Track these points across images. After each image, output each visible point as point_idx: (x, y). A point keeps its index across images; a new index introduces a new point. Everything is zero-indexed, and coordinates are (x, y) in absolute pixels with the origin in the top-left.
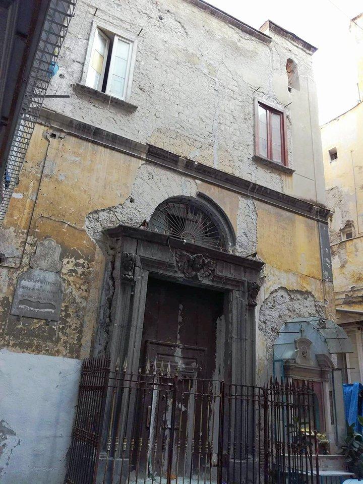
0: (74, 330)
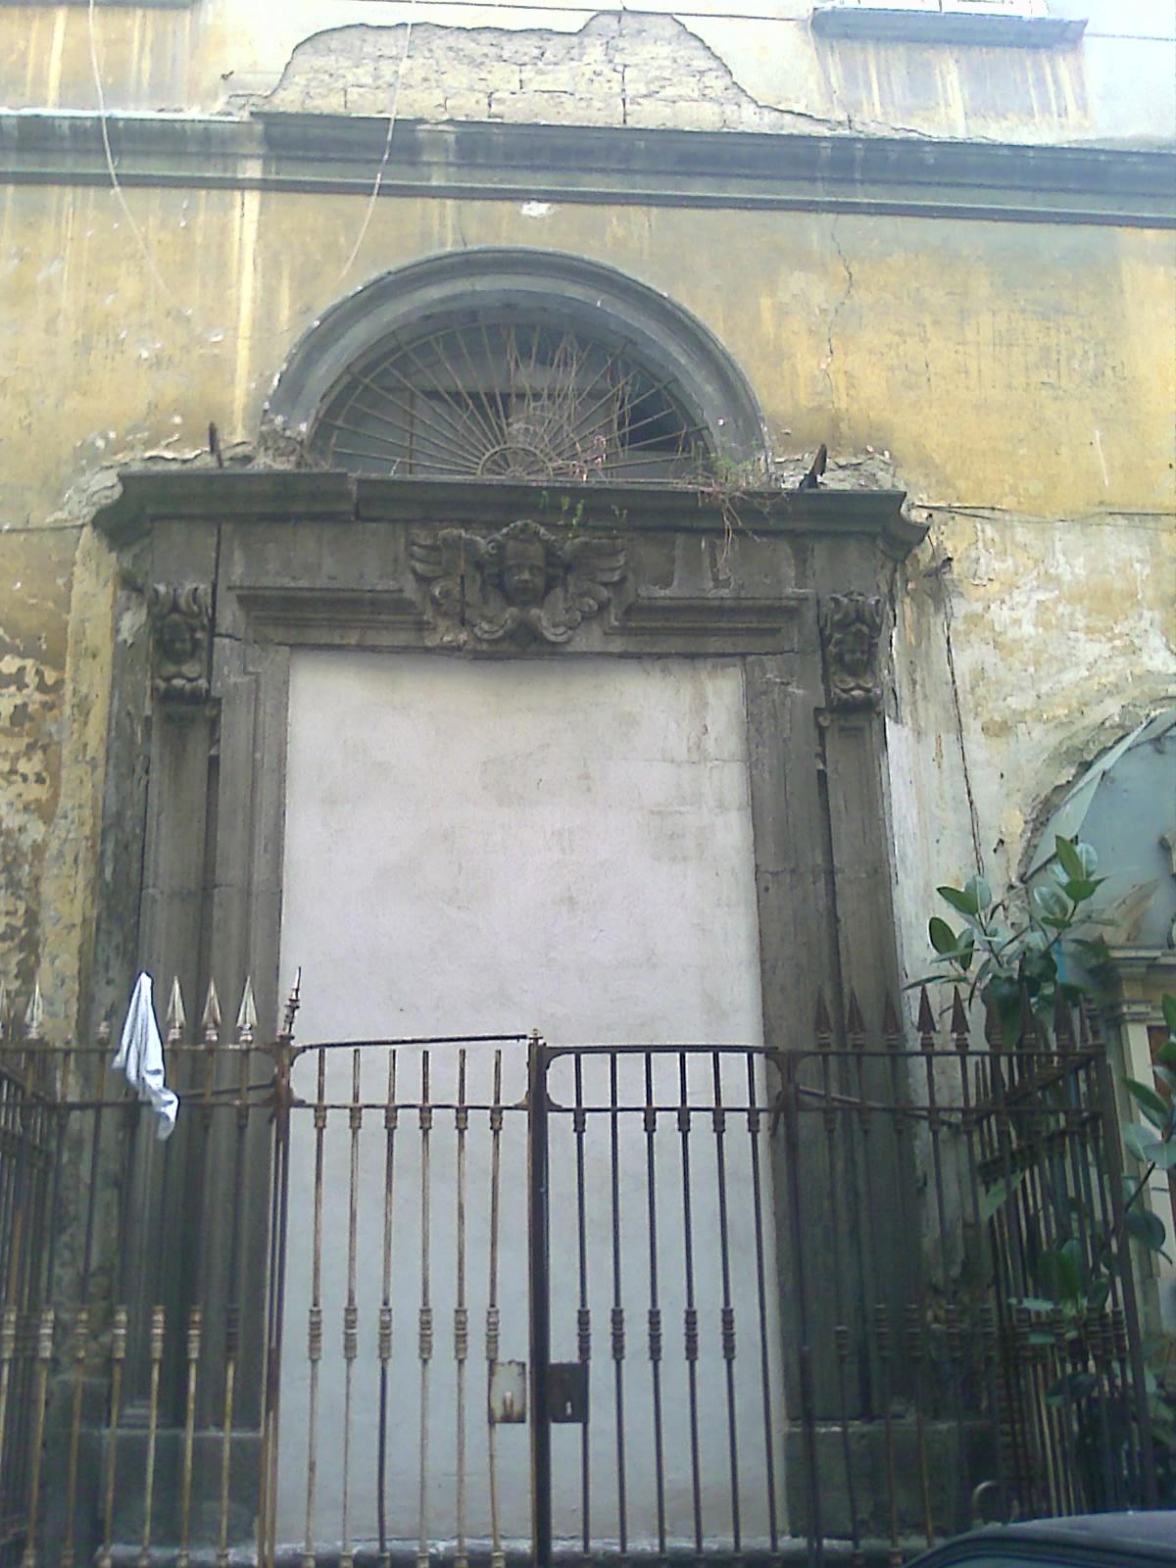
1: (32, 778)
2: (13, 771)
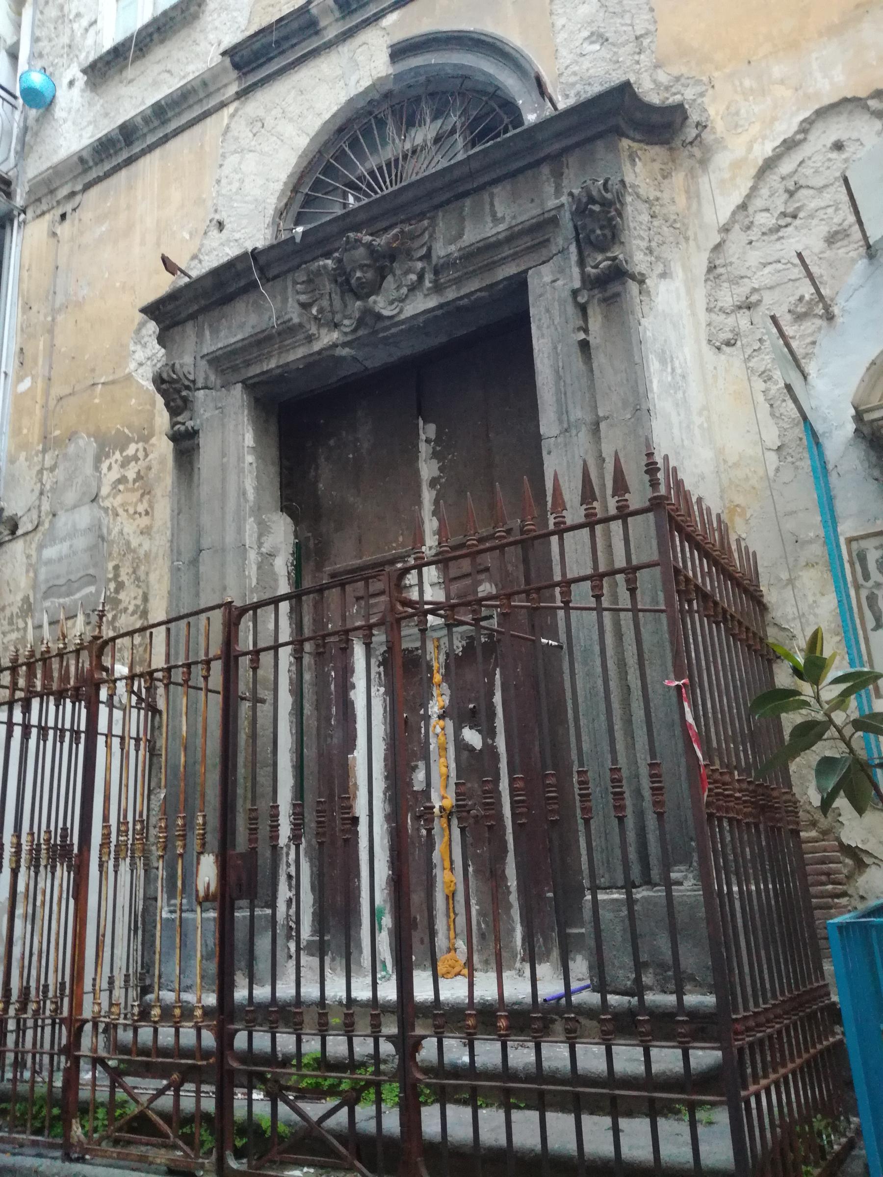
0: (133, 614)
1: (143, 513)
2: (135, 513)
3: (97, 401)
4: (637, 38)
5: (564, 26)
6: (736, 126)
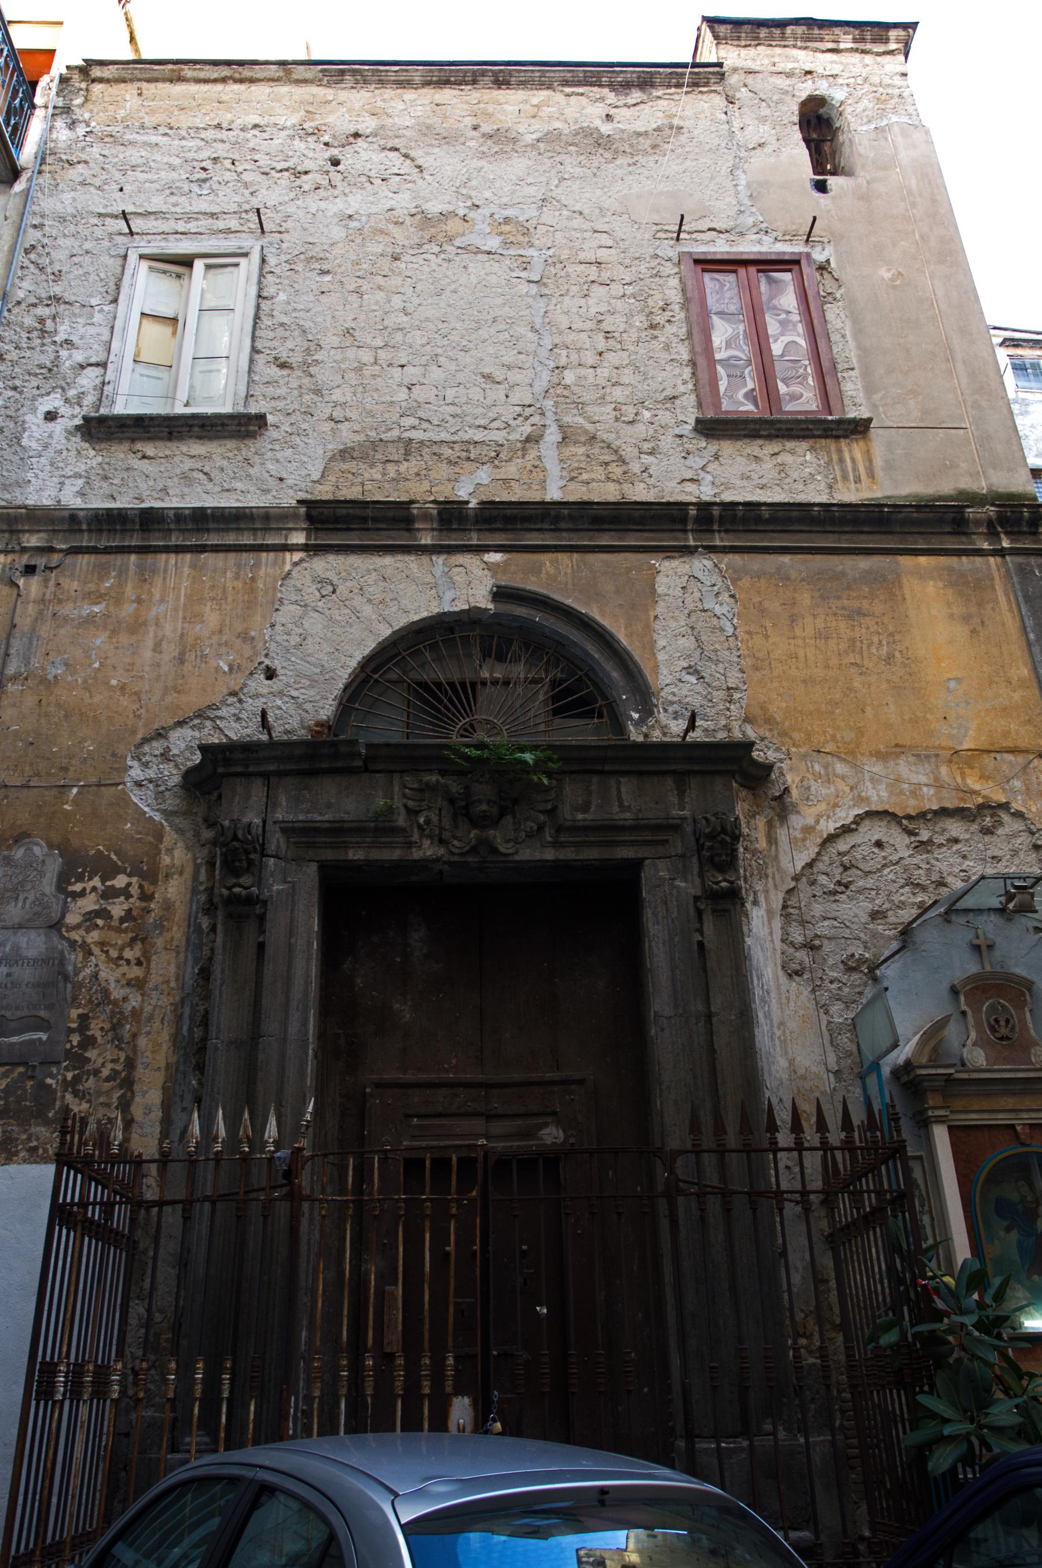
0: (108, 1079)
1: (133, 962)
2: (120, 958)
3: (67, 807)
4: (729, 689)
5: (665, 647)
6: (808, 799)
